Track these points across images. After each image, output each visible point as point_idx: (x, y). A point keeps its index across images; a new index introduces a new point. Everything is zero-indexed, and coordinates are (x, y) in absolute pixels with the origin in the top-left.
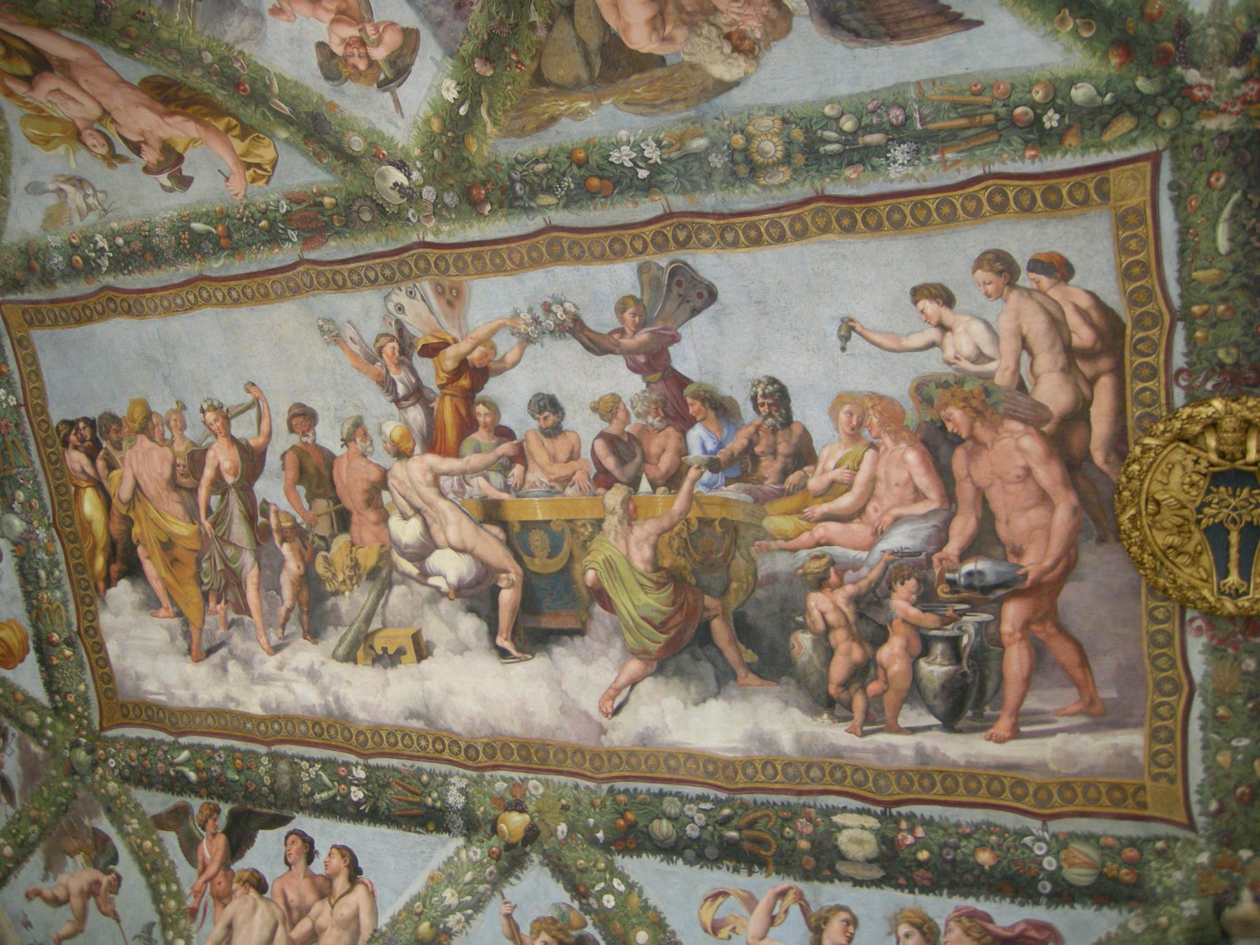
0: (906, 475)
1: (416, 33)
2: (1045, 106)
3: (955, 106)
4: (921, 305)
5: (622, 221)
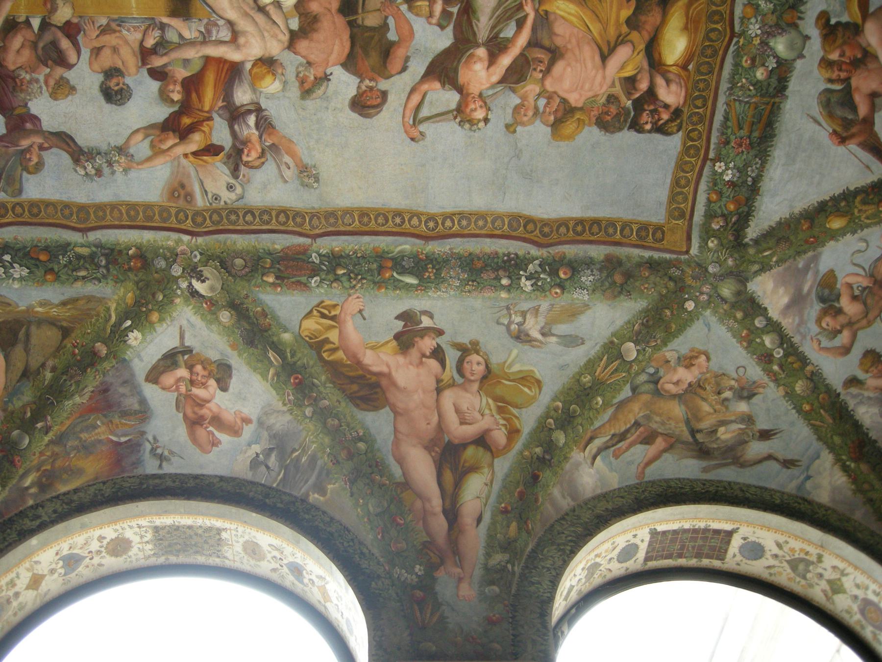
1: (147, 379)
5: (27, 228)
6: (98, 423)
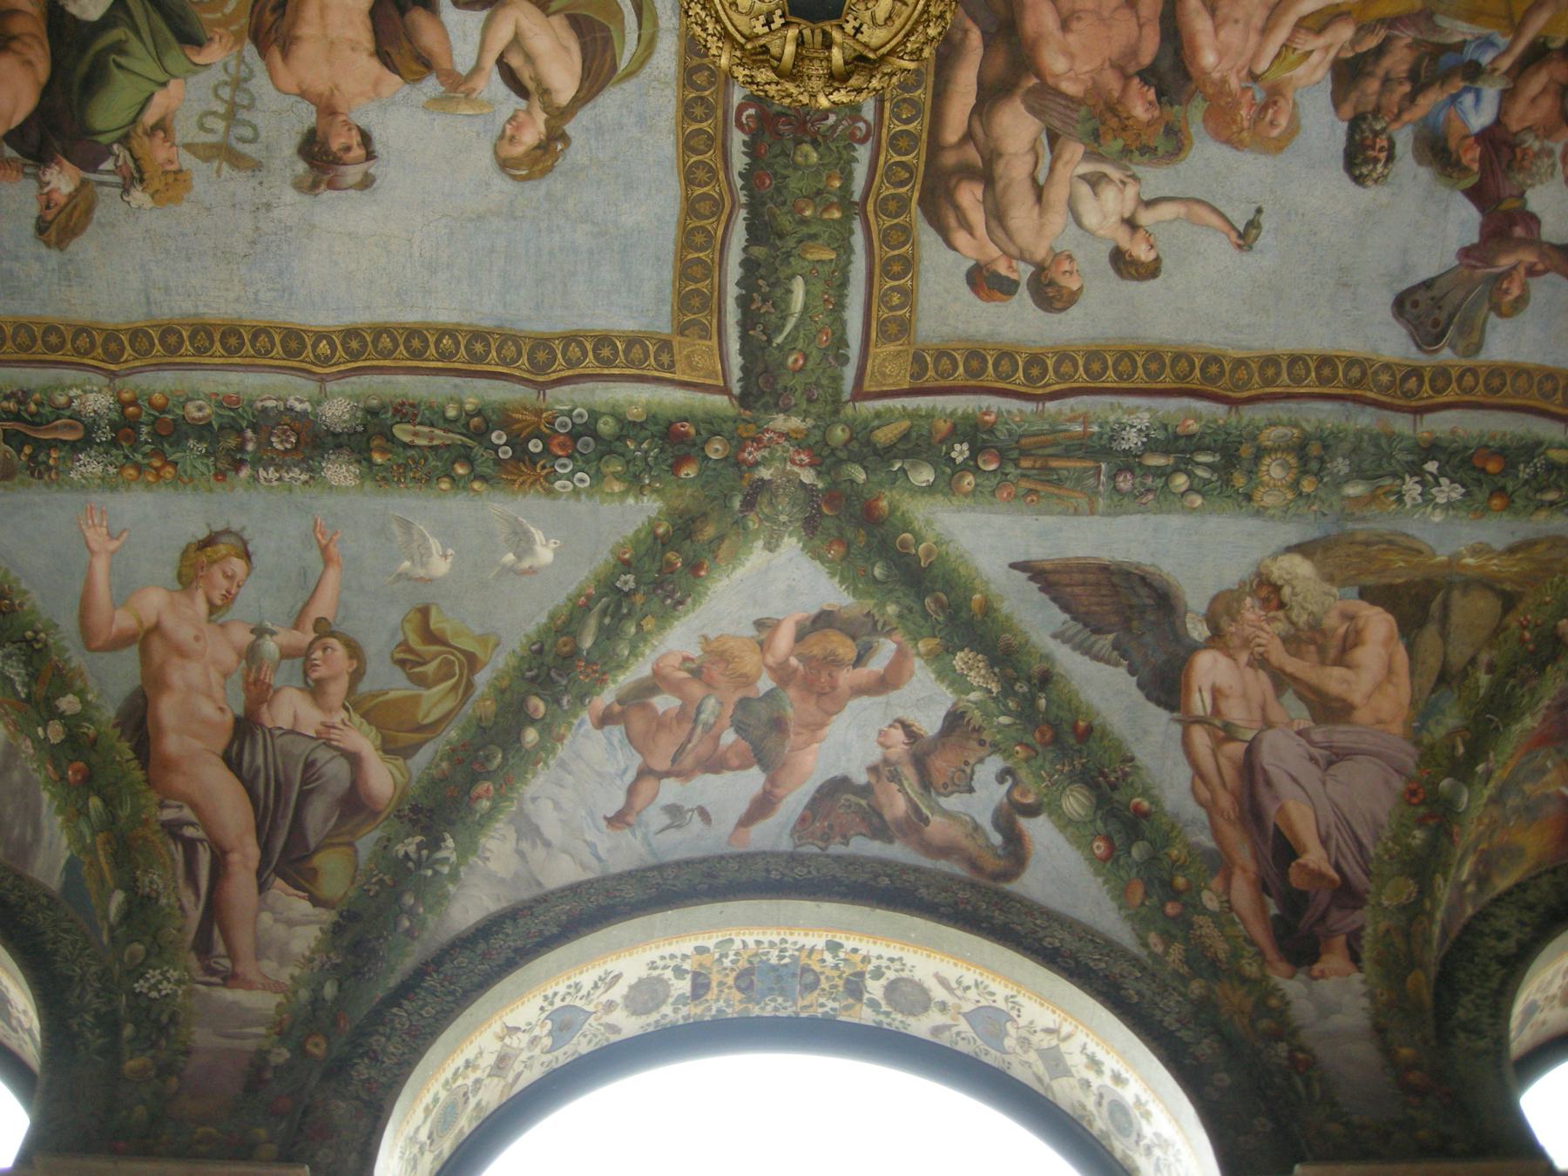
0: (1222, 34)
2: (964, 468)
3: (1059, 483)
4: (1152, 256)
6: (1549, 764)
